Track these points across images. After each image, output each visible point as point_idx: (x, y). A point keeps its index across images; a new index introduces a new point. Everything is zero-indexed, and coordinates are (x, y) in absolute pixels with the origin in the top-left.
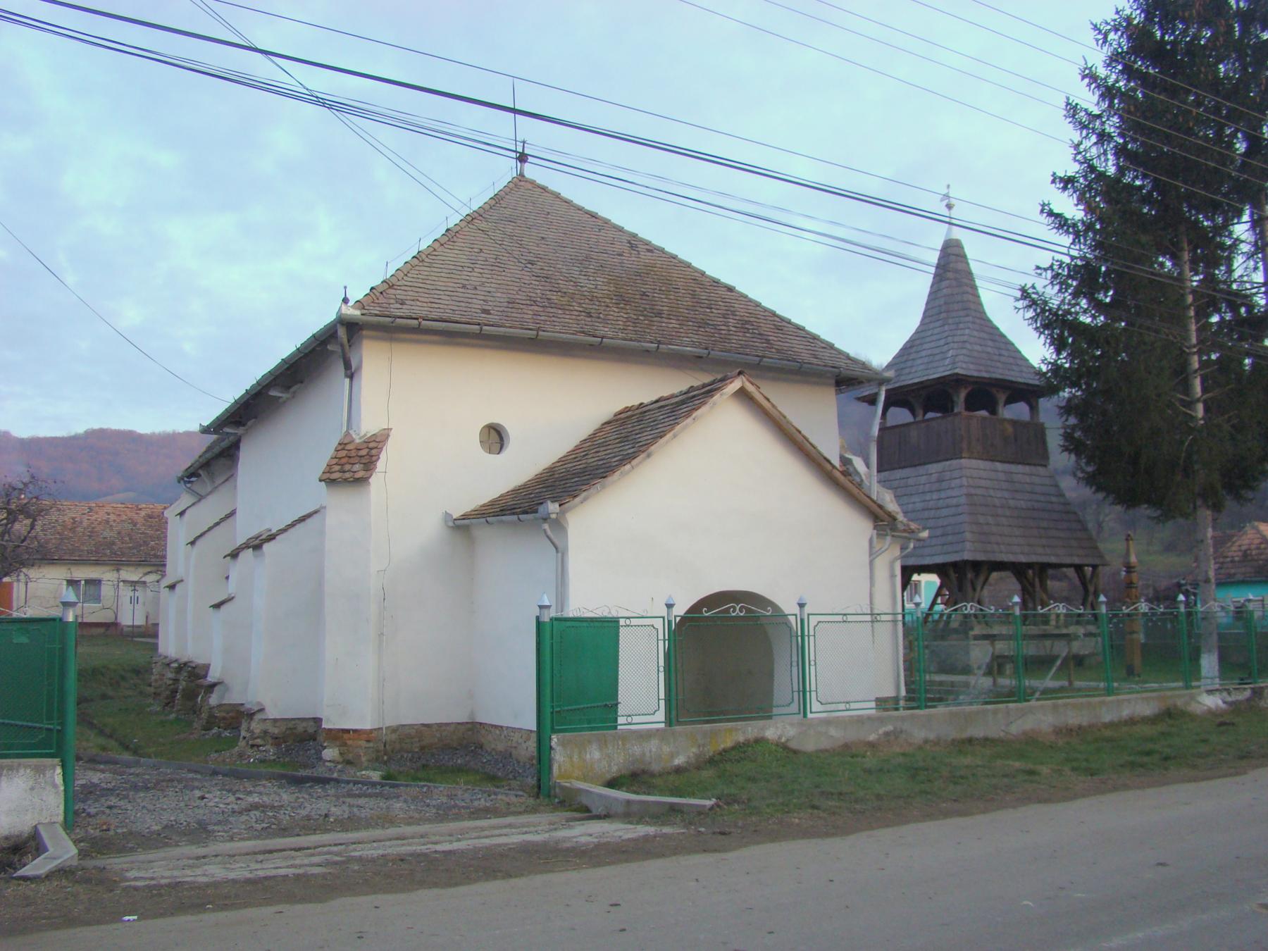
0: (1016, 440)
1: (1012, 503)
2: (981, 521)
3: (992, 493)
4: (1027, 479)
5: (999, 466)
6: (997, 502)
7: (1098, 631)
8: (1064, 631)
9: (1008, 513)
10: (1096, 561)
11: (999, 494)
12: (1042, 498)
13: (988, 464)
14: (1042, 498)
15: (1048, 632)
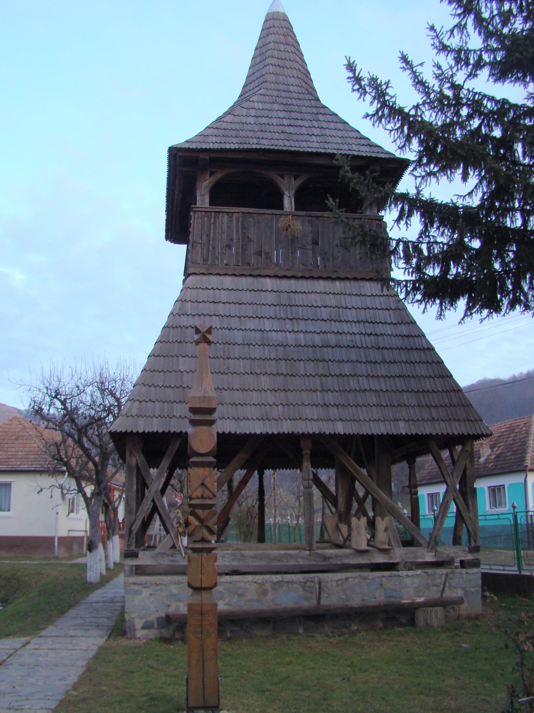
0: (315, 243)
1: (275, 337)
2: (182, 368)
3: (234, 323)
4: (331, 300)
5: (269, 283)
6: (238, 337)
7: (470, 557)
8: (380, 559)
9: (256, 352)
10: (457, 429)
11: (252, 324)
12: (355, 328)
13: (246, 282)
14: (355, 328)
15: (334, 562)
